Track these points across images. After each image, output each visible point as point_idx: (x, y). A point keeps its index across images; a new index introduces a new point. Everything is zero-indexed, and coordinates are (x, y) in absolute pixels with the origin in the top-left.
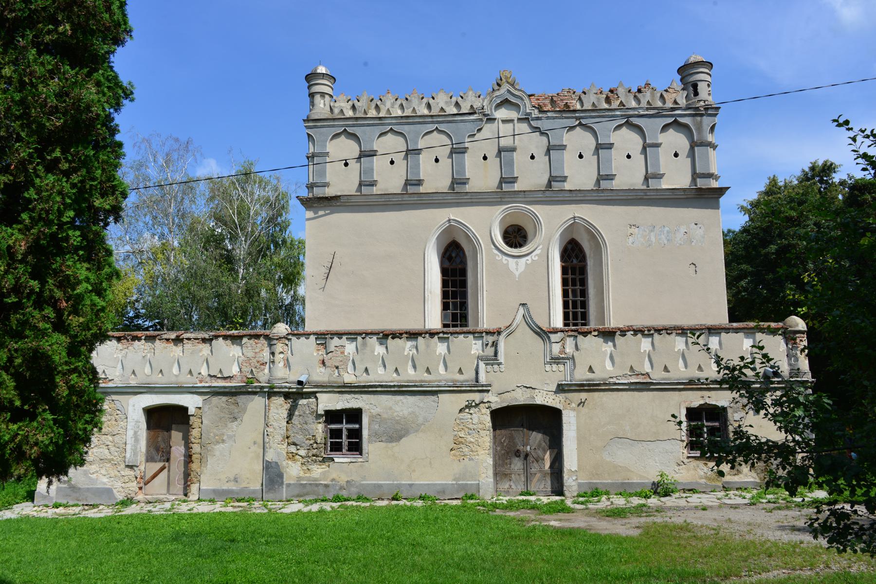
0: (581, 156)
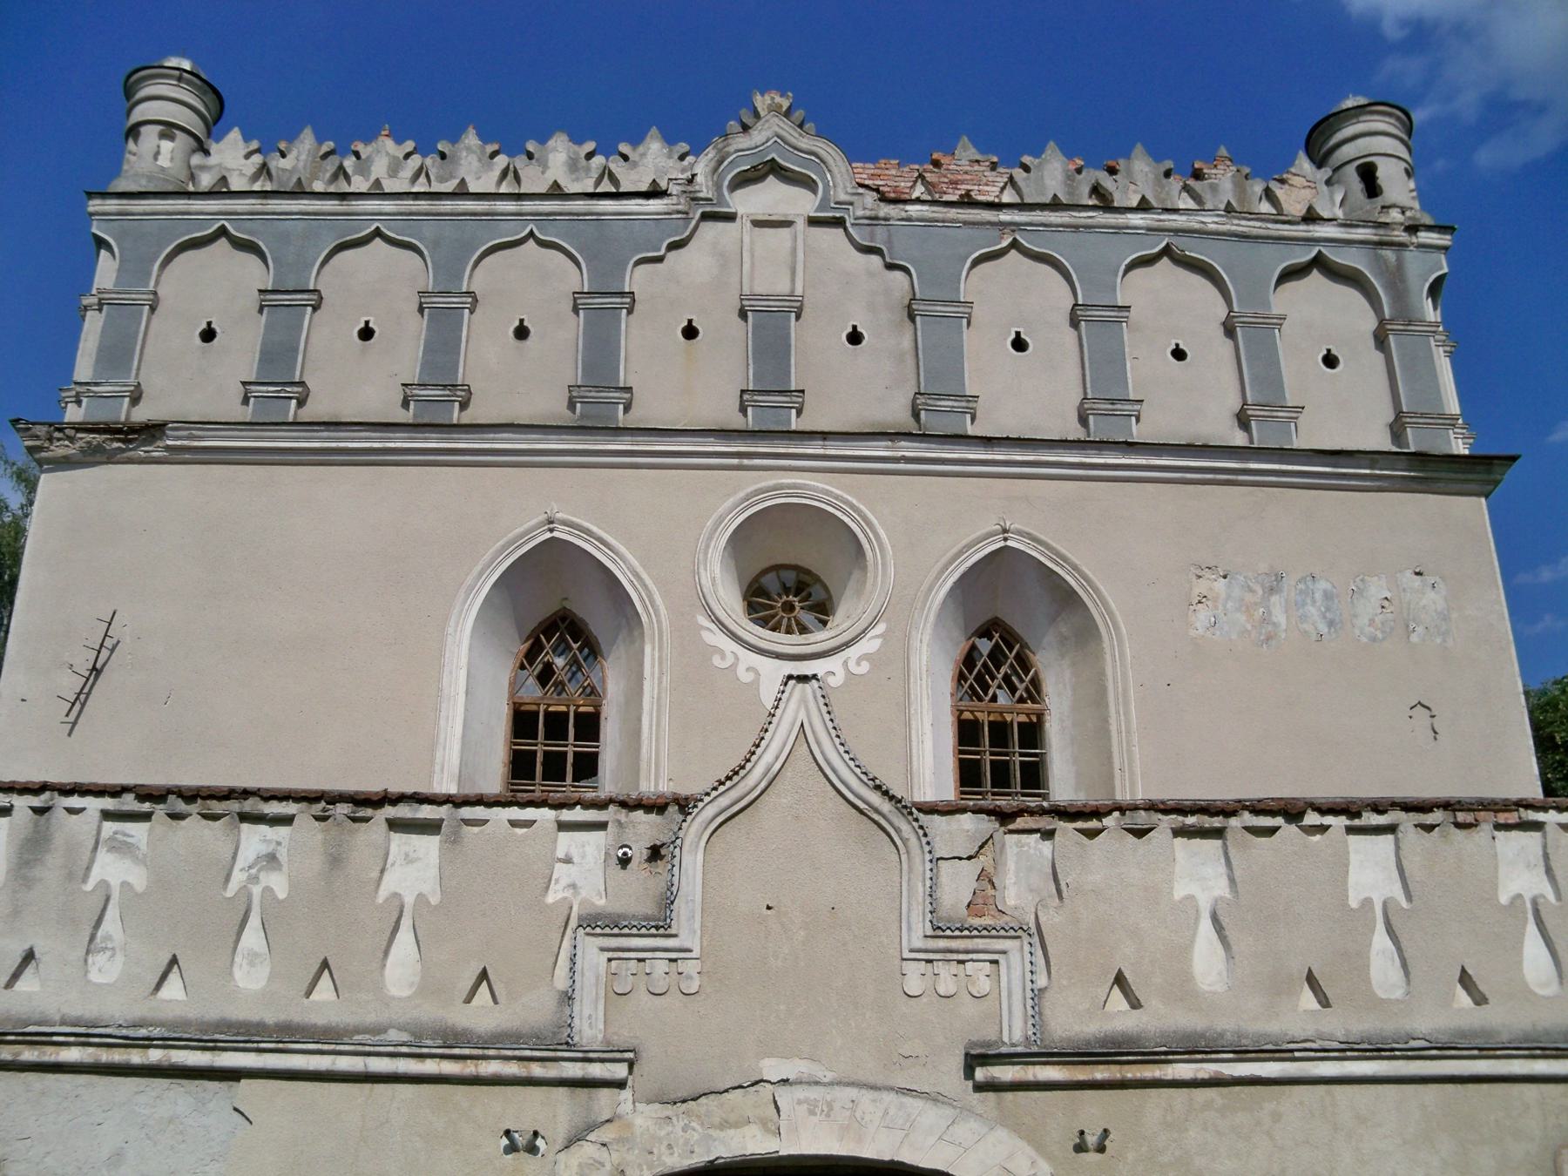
0: (1019, 344)
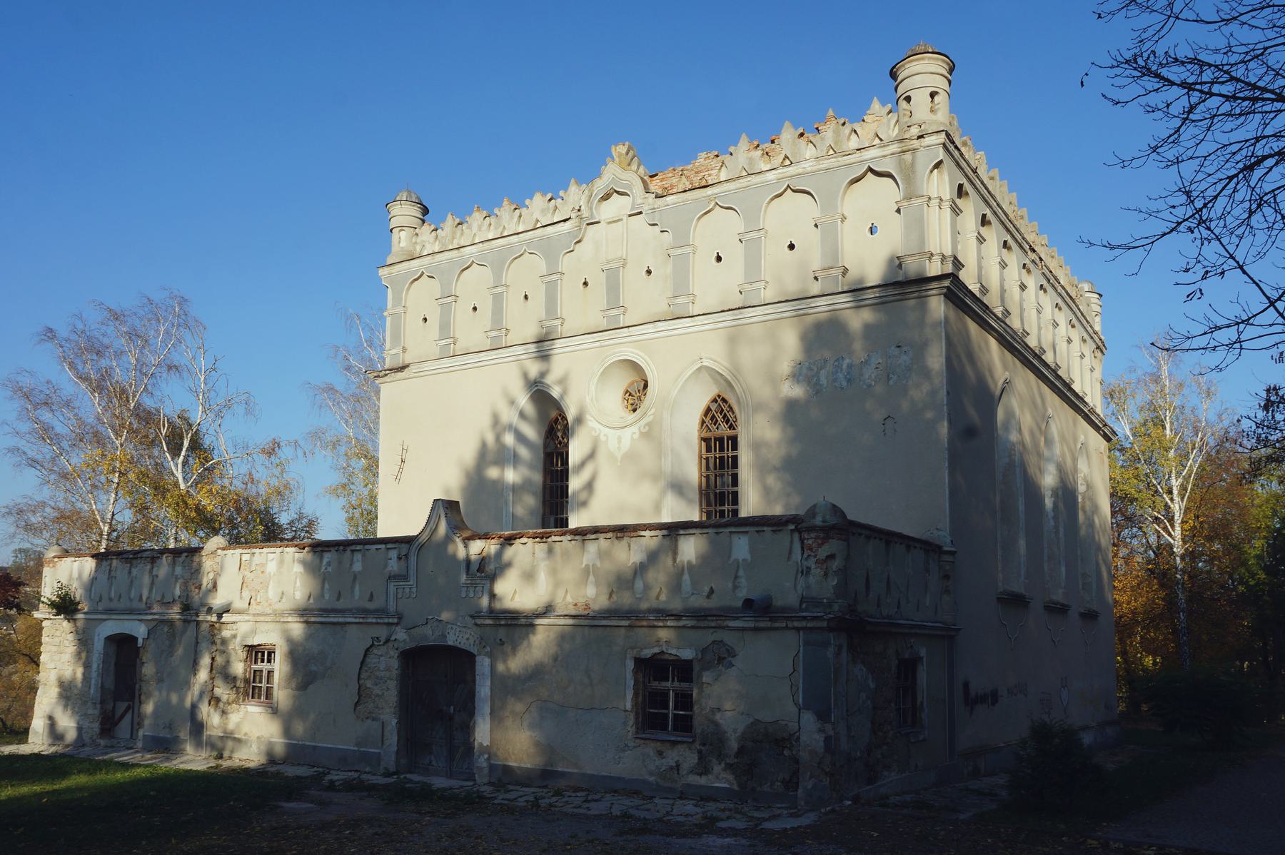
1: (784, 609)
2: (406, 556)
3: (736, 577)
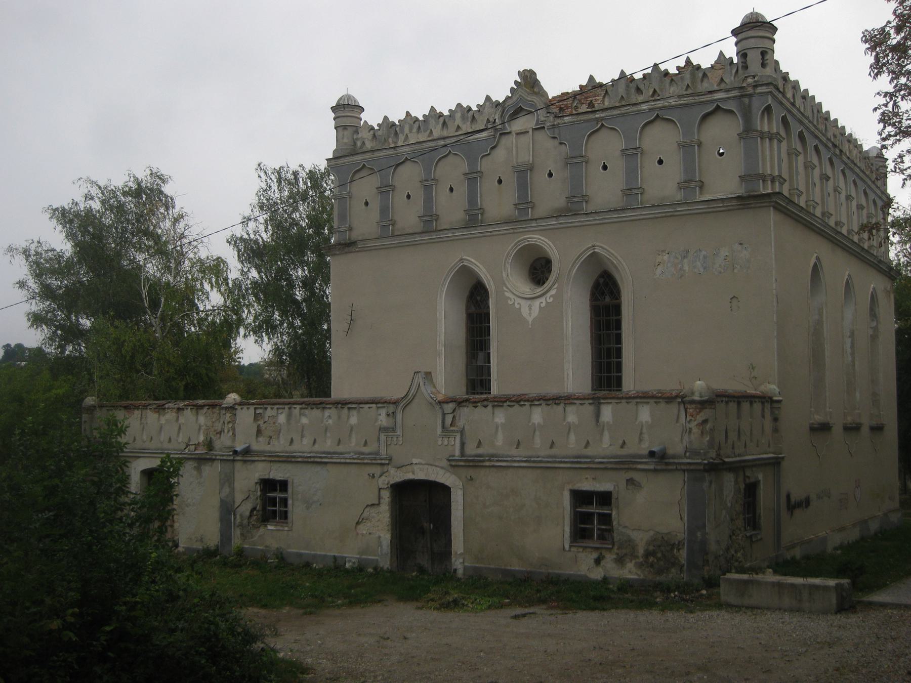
0: (605, 167)
1: (674, 457)
2: (394, 413)
3: (641, 433)
